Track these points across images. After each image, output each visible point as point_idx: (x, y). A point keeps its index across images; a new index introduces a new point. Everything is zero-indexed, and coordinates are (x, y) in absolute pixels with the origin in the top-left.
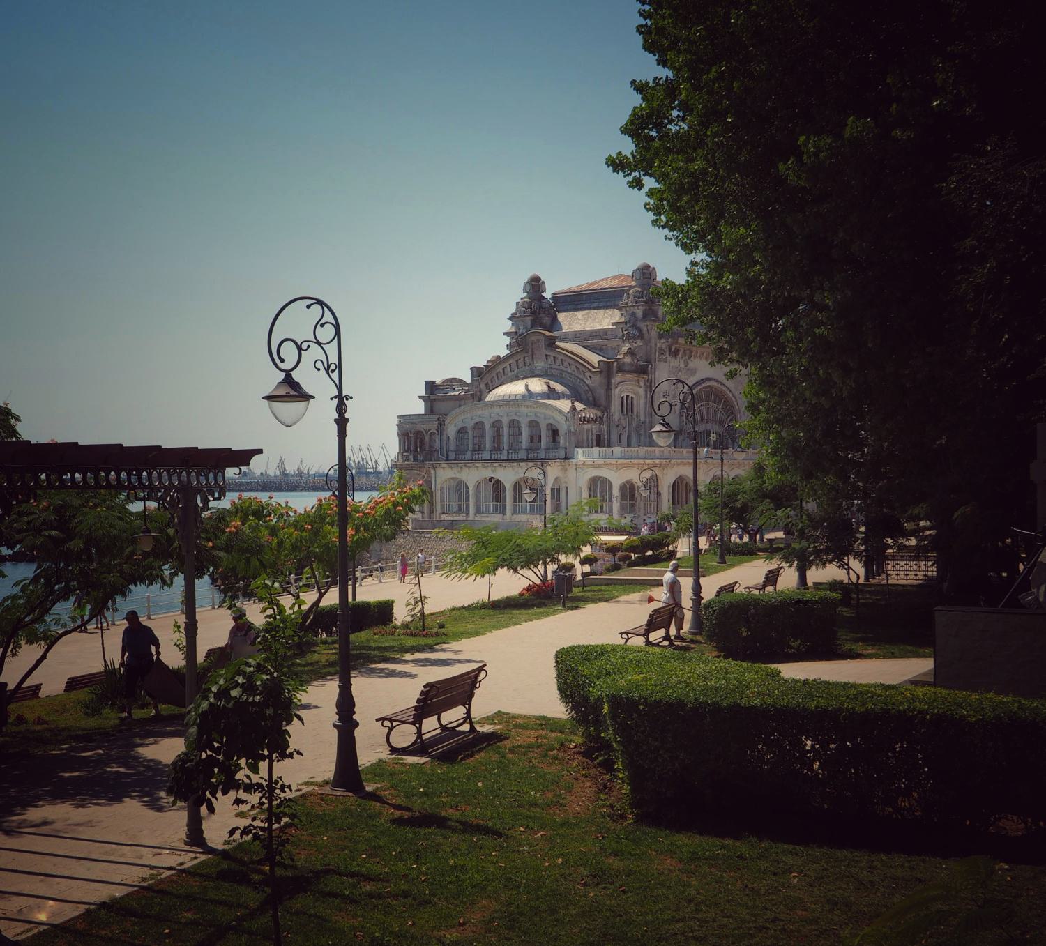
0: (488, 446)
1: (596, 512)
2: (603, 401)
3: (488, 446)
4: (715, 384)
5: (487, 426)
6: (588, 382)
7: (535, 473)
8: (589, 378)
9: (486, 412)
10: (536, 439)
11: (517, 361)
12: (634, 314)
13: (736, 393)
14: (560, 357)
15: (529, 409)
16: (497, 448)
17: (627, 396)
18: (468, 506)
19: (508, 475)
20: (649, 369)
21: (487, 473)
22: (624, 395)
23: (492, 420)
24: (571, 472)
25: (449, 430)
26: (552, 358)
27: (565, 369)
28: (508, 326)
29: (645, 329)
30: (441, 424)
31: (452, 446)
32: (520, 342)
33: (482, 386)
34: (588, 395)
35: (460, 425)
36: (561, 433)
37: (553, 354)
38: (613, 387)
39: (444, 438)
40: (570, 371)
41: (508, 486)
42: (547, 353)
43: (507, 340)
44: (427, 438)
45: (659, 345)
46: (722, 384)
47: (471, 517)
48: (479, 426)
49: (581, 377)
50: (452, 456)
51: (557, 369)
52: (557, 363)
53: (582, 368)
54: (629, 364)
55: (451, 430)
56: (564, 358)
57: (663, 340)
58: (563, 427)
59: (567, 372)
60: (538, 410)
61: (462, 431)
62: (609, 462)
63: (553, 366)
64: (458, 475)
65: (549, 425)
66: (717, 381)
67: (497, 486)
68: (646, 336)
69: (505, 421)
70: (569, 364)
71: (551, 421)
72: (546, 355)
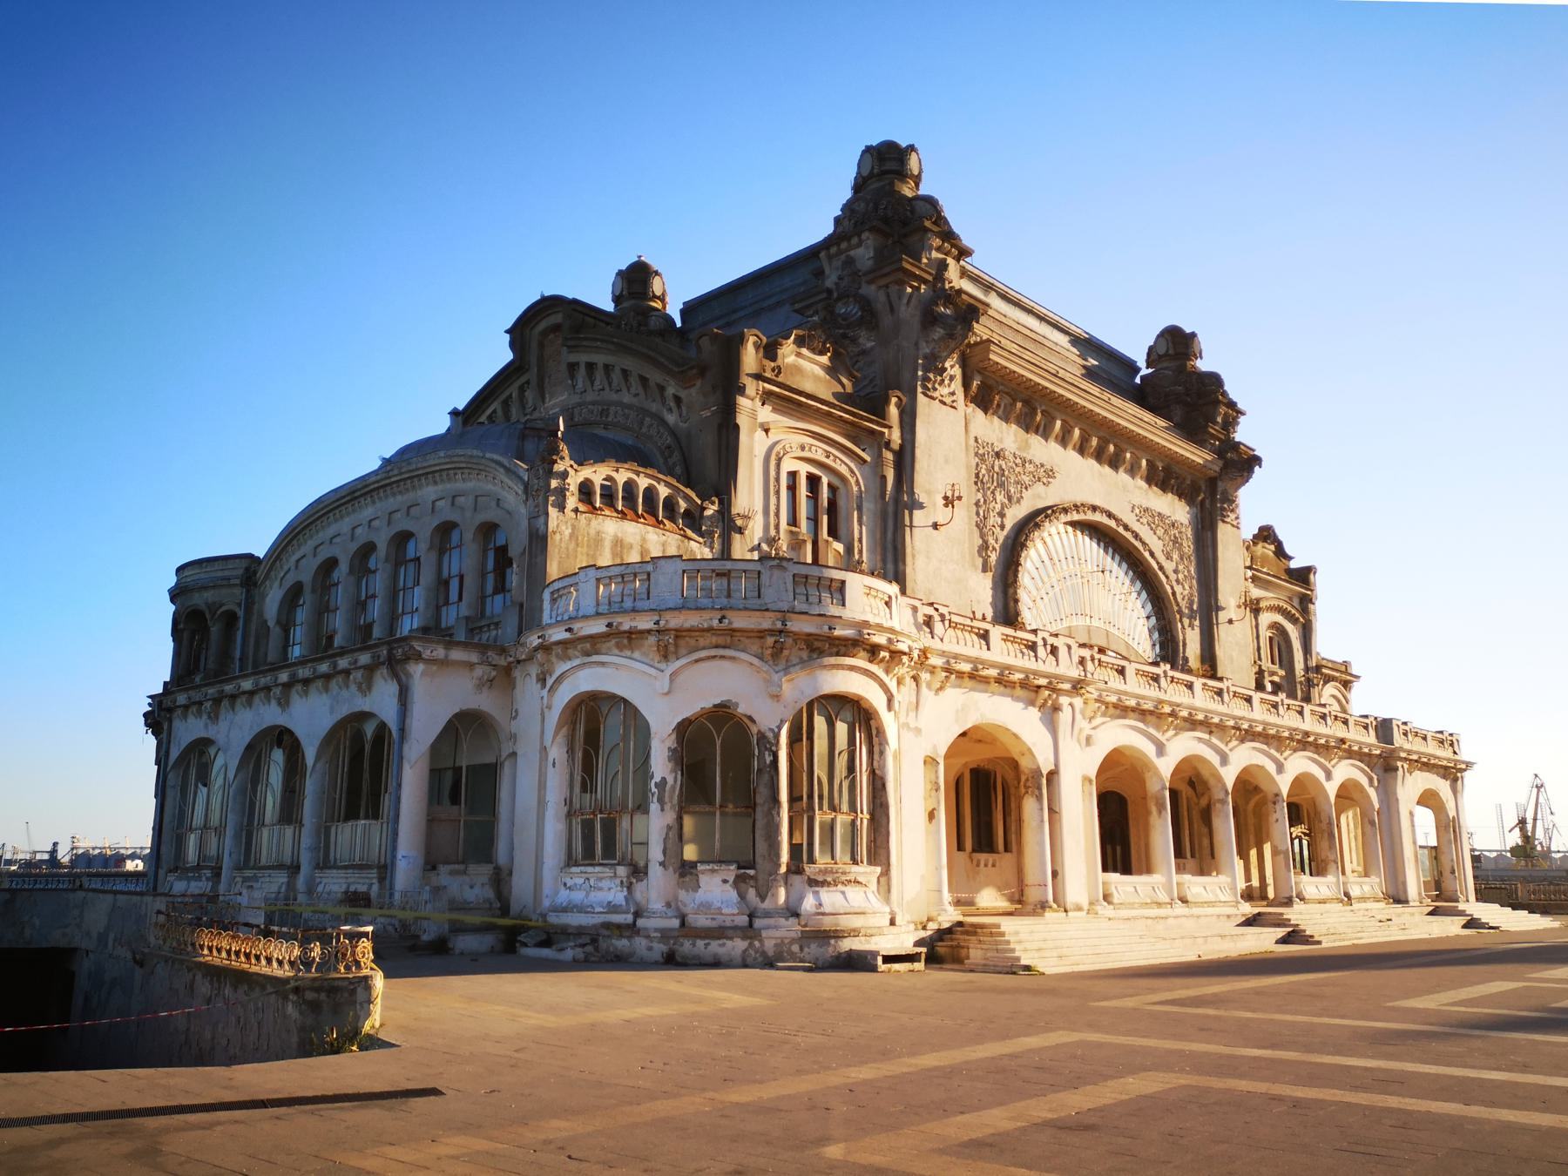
1: (589, 856)
4: (1112, 524)
6: (671, 419)
7: (382, 700)
8: (672, 404)
11: (506, 404)
12: (850, 262)
13: (1169, 566)
14: (600, 359)
15: (440, 487)
17: (813, 481)
20: (893, 411)
22: (804, 469)
23: (354, 547)
25: (268, 600)
26: (582, 370)
27: (614, 397)
29: (882, 297)
34: (671, 461)
35: (290, 581)
37: (583, 358)
38: (742, 420)
39: (253, 627)
40: (627, 398)
42: (573, 358)
45: (925, 349)
46: (1126, 528)
49: (654, 407)
51: (593, 403)
52: (597, 383)
53: (655, 376)
54: (816, 378)
56: (610, 359)
57: (939, 332)
59: (620, 404)
60: (459, 485)
61: (294, 595)
62: (626, 627)
63: (590, 397)
65: (488, 530)
66: (1110, 515)
68: (886, 320)
70: (625, 373)
71: (491, 515)
72: (573, 367)
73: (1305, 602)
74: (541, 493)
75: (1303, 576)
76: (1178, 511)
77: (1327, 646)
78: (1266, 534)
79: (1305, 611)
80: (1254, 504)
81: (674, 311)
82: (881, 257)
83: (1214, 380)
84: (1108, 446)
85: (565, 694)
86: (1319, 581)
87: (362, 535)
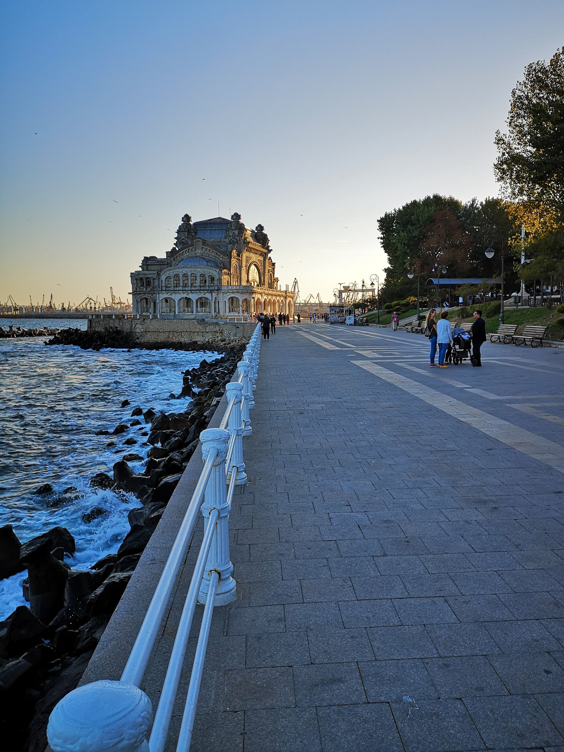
0: (181, 285)
1: (233, 311)
2: (228, 267)
3: (181, 285)
5: (181, 276)
7: (208, 296)
9: (181, 270)
10: (204, 282)
12: (234, 233)
16: (185, 285)
18: (175, 310)
19: (194, 297)
21: (185, 295)
24: (221, 295)
28: (176, 235)
30: (159, 275)
31: (164, 285)
32: (180, 241)
33: (172, 259)
35: (168, 275)
36: (215, 279)
41: (194, 301)
43: (175, 241)
44: (152, 281)
47: (177, 314)
48: (177, 276)
50: (164, 288)
55: (163, 278)
58: (217, 277)
61: (168, 278)
64: (170, 296)
67: (188, 300)
69: (189, 274)
73: (274, 269)
74: (220, 274)
75: (274, 264)
76: (261, 258)
77: (276, 276)
78: (270, 258)
79: (274, 270)
80: (269, 255)
81: (192, 223)
82: (239, 234)
83: (266, 235)
84: (256, 252)
85: (229, 296)
86: (276, 265)
87: (184, 272)
